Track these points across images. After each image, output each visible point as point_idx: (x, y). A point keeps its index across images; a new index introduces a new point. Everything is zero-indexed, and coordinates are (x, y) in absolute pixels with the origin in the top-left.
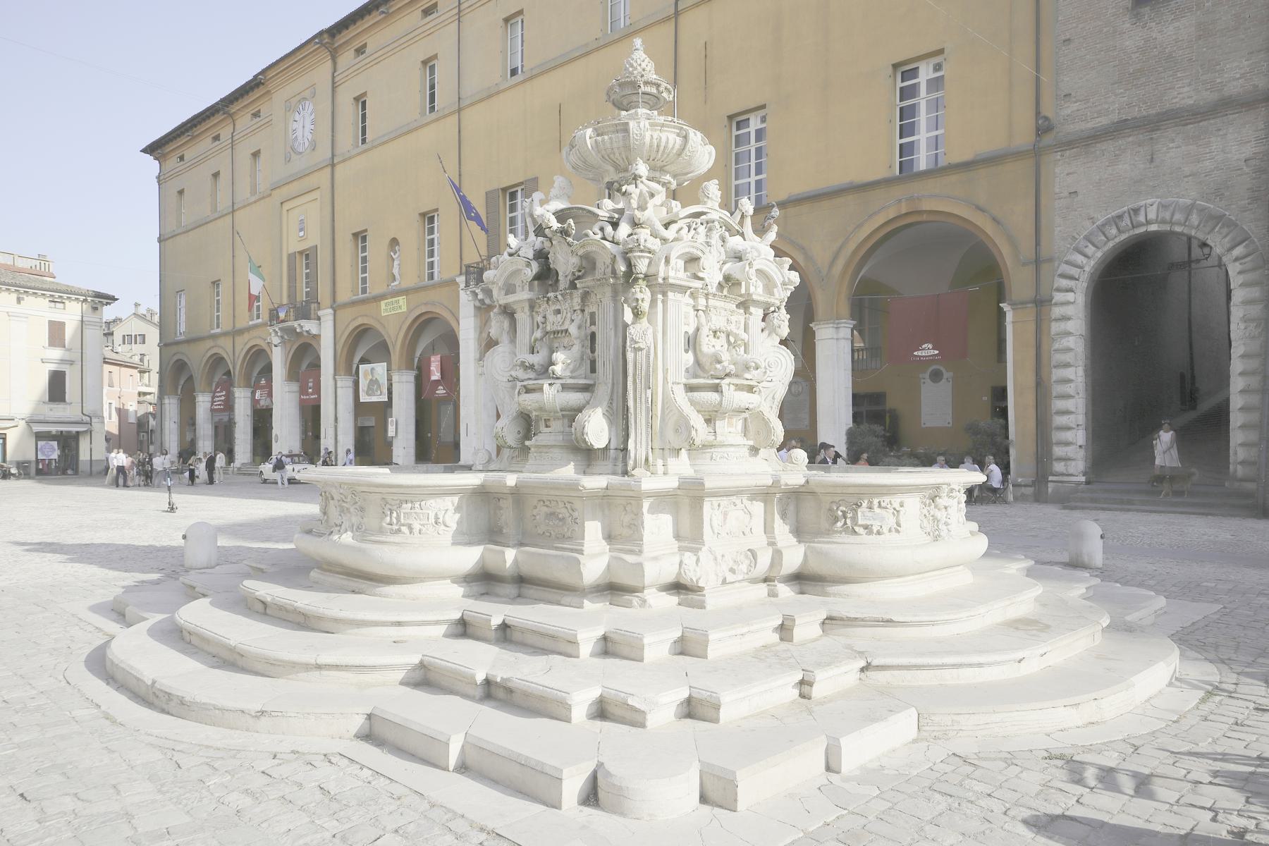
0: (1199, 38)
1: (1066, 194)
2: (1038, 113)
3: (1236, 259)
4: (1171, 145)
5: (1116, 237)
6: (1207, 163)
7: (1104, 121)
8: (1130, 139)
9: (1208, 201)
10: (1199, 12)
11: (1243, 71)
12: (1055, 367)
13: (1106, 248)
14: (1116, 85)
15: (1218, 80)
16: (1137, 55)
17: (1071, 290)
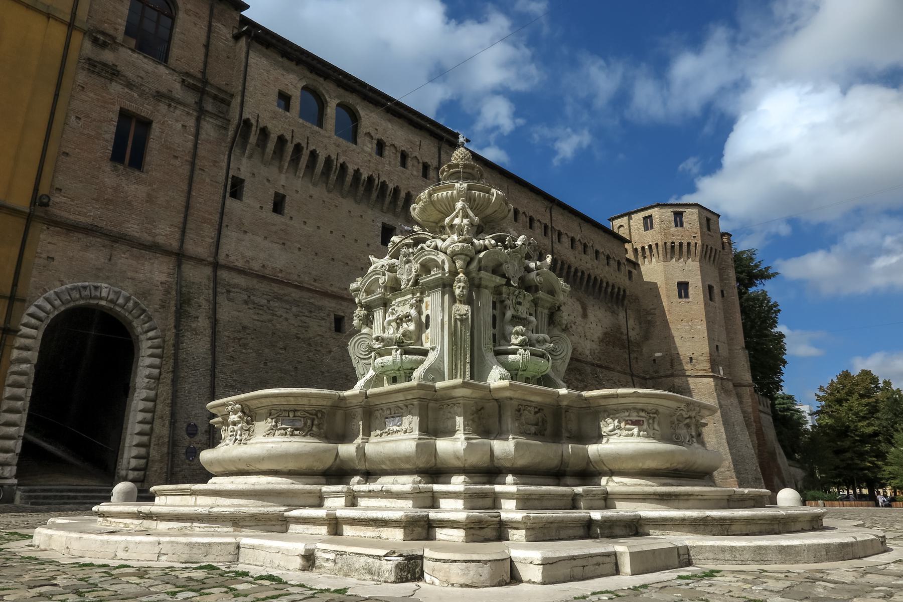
0: (147, 202)
1: (44, 255)
2: (36, 189)
3: (150, 339)
4: (123, 255)
5: (77, 300)
6: (141, 275)
7: (82, 219)
8: (99, 240)
9: (138, 298)
10: (149, 188)
11: (166, 232)
12: (9, 386)
13: (68, 306)
14: (94, 201)
15: (153, 231)
16: (111, 190)
17: (36, 328)
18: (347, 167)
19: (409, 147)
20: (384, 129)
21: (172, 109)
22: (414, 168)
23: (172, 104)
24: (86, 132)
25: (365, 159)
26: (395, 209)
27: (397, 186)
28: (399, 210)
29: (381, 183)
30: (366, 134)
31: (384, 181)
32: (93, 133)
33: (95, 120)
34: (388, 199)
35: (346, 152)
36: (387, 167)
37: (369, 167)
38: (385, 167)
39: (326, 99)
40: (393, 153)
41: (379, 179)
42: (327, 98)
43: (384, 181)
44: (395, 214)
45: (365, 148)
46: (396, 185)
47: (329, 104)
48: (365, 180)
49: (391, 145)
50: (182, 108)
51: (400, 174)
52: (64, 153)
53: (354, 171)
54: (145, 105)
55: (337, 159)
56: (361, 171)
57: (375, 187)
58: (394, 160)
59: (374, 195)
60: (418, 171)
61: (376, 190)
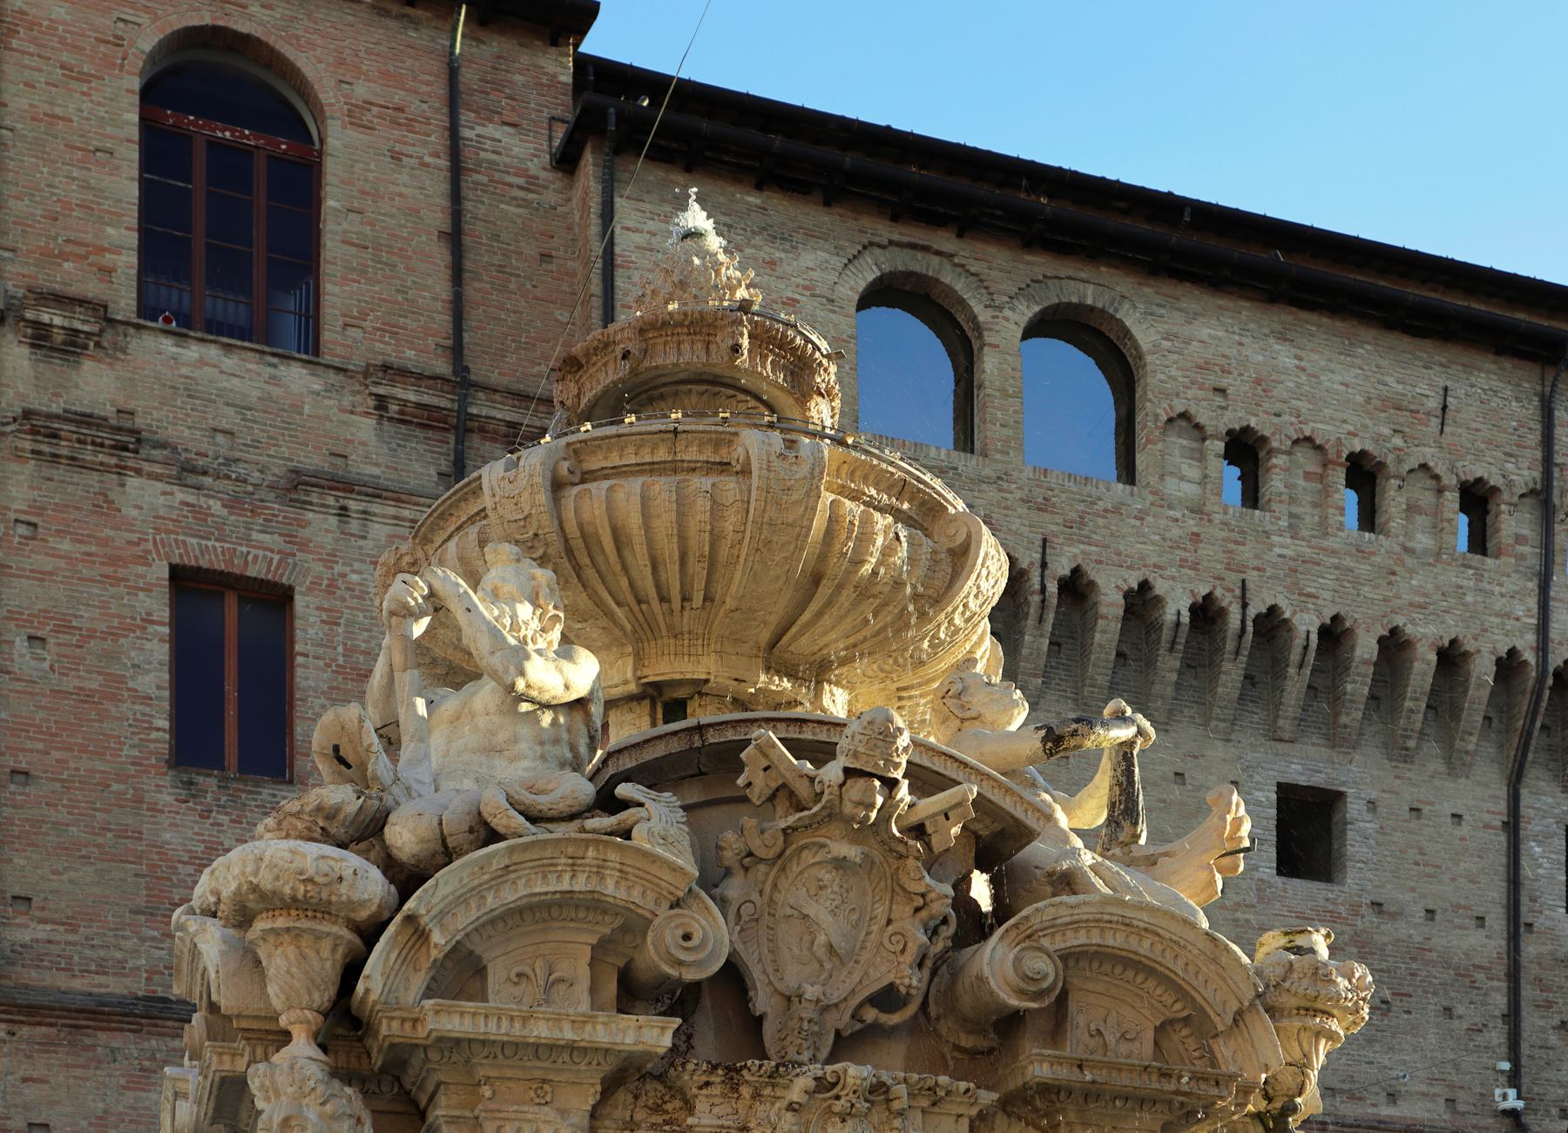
18: (1092, 584)
19: (1386, 431)
20: (1258, 382)
21: (354, 526)
22: (1419, 519)
23: (352, 505)
24: (70, 683)
25: (1176, 532)
26: (1337, 715)
27: (1336, 619)
28: (1352, 716)
29: (1258, 619)
30: (1170, 420)
31: (1273, 610)
32: (94, 683)
33: (91, 634)
34: (1295, 684)
35: (1083, 523)
36: (1284, 546)
37: (1195, 567)
38: (1271, 546)
39: (974, 318)
40: (1308, 476)
41: (1245, 606)
42: (977, 308)
43: (1273, 610)
44: (1336, 738)
45: (1172, 487)
46: (1327, 615)
47: (989, 337)
48: (1178, 624)
49: (1296, 442)
50: (392, 511)
51: (1348, 562)
52: (14, 772)
53: (1128, 595)
54: (255, 535)
55: (1044, 565)
56: (1160, 587)
57: (1230, 645)
58: (1315, 505)
59: (1231, 674)
60: (1437, 530)
61: (1237, 653)
